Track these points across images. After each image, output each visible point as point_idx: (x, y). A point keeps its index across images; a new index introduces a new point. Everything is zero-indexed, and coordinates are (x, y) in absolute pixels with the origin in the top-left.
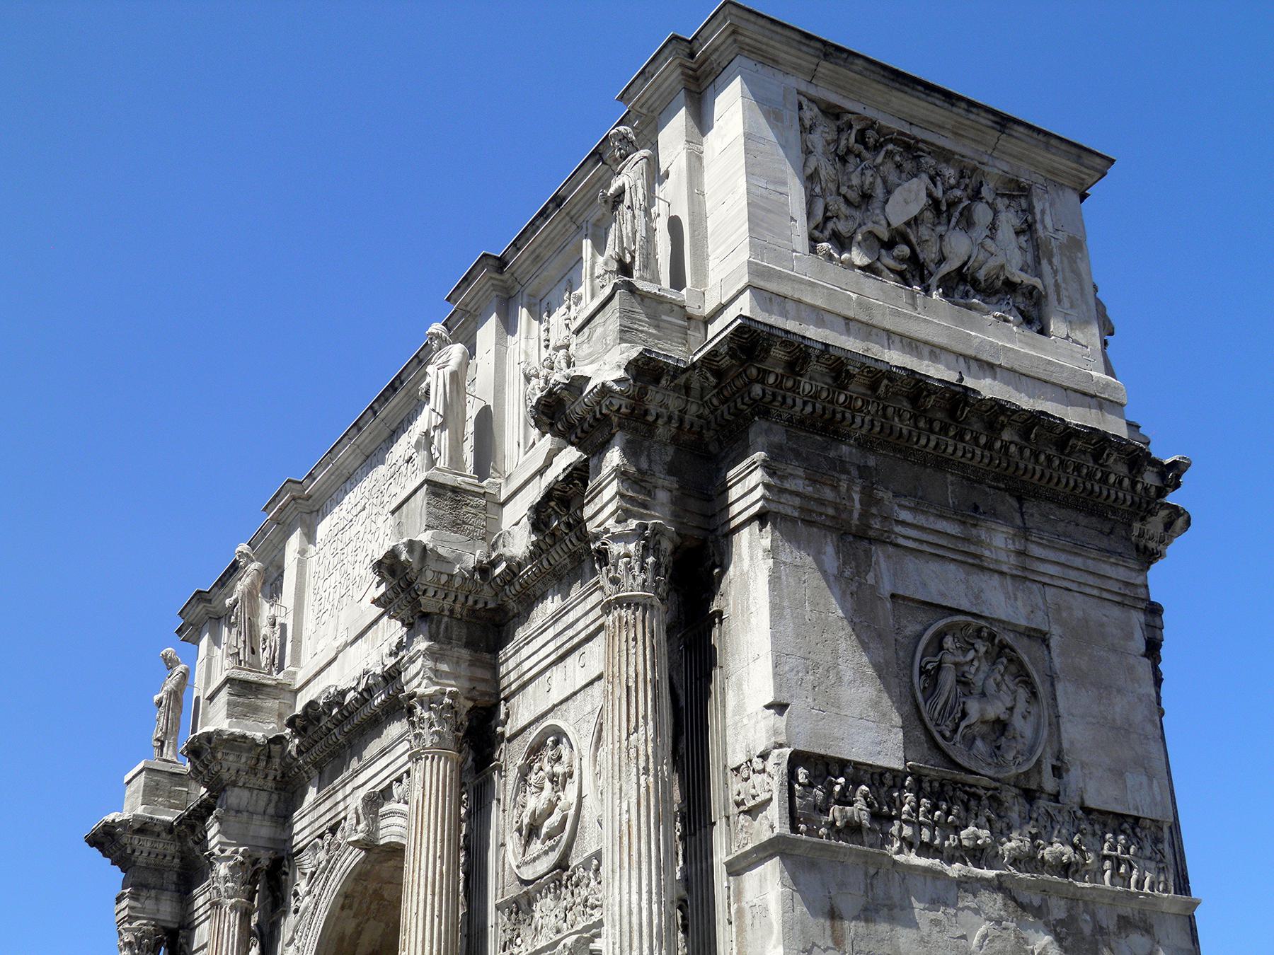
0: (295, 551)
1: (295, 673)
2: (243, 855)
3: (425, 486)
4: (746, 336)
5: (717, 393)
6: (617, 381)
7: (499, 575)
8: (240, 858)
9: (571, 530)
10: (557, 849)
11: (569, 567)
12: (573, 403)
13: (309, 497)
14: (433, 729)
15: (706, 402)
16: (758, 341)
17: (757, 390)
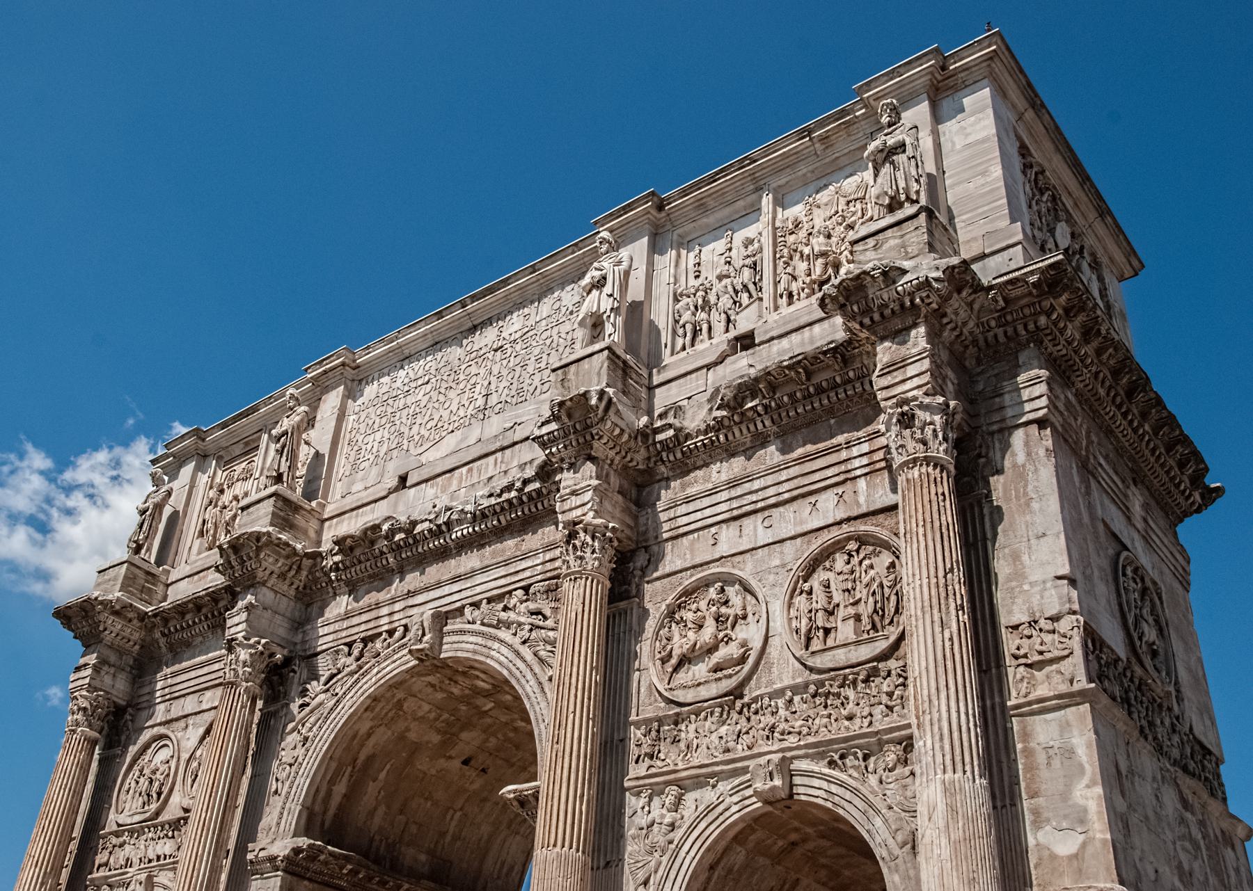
0: (334, 408)
1: (324, 505)
2: (264, 646)
3: (606, 352)
4: (1052, 273)
5: (1000, 317)
6: (936, 280)
7: (661, 442)
8: (260, 648)
9: (766, 413)
10: (734, 678)
11: (748, 445)
12: (881, 289)
13: (358, 367)
14: (595, 555)
15: (982, 324)
16: (1061, 280)
17: (1043, 320)
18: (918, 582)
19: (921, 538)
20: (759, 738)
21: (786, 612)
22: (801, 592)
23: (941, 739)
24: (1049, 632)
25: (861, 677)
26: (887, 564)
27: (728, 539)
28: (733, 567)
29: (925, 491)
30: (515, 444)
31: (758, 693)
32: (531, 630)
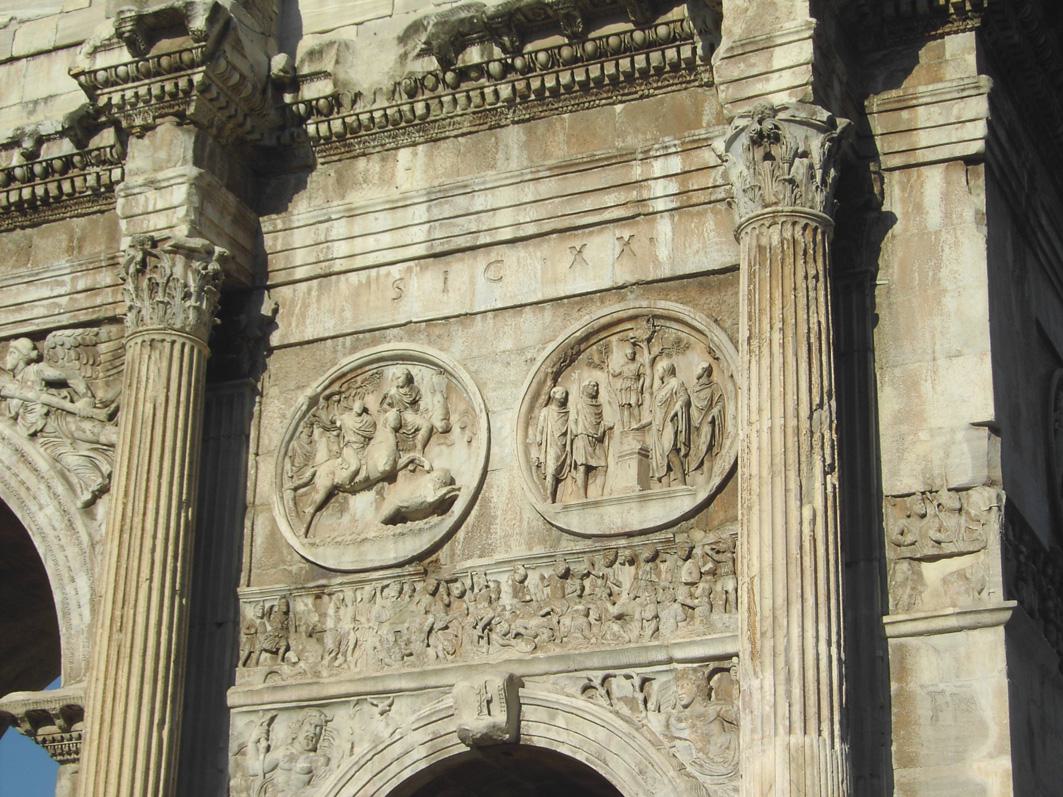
14: (188, 304)
18: (766, 424)
19: (776, 349)
20: (466, 640)
21: (521, 433)
22: (549, 400)
23: (789, 680)
24: (953, 510)
25: (646, 554)
26: (699, 371)
27: (425, 294)
28: (430, 343)
29: (788, 270)
30: (12, 60)
31: (468, 563)
32: (47, 414)
